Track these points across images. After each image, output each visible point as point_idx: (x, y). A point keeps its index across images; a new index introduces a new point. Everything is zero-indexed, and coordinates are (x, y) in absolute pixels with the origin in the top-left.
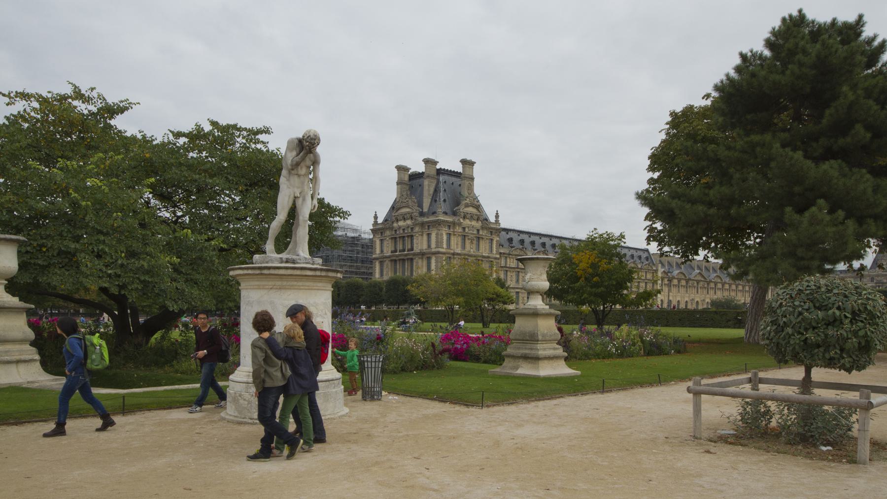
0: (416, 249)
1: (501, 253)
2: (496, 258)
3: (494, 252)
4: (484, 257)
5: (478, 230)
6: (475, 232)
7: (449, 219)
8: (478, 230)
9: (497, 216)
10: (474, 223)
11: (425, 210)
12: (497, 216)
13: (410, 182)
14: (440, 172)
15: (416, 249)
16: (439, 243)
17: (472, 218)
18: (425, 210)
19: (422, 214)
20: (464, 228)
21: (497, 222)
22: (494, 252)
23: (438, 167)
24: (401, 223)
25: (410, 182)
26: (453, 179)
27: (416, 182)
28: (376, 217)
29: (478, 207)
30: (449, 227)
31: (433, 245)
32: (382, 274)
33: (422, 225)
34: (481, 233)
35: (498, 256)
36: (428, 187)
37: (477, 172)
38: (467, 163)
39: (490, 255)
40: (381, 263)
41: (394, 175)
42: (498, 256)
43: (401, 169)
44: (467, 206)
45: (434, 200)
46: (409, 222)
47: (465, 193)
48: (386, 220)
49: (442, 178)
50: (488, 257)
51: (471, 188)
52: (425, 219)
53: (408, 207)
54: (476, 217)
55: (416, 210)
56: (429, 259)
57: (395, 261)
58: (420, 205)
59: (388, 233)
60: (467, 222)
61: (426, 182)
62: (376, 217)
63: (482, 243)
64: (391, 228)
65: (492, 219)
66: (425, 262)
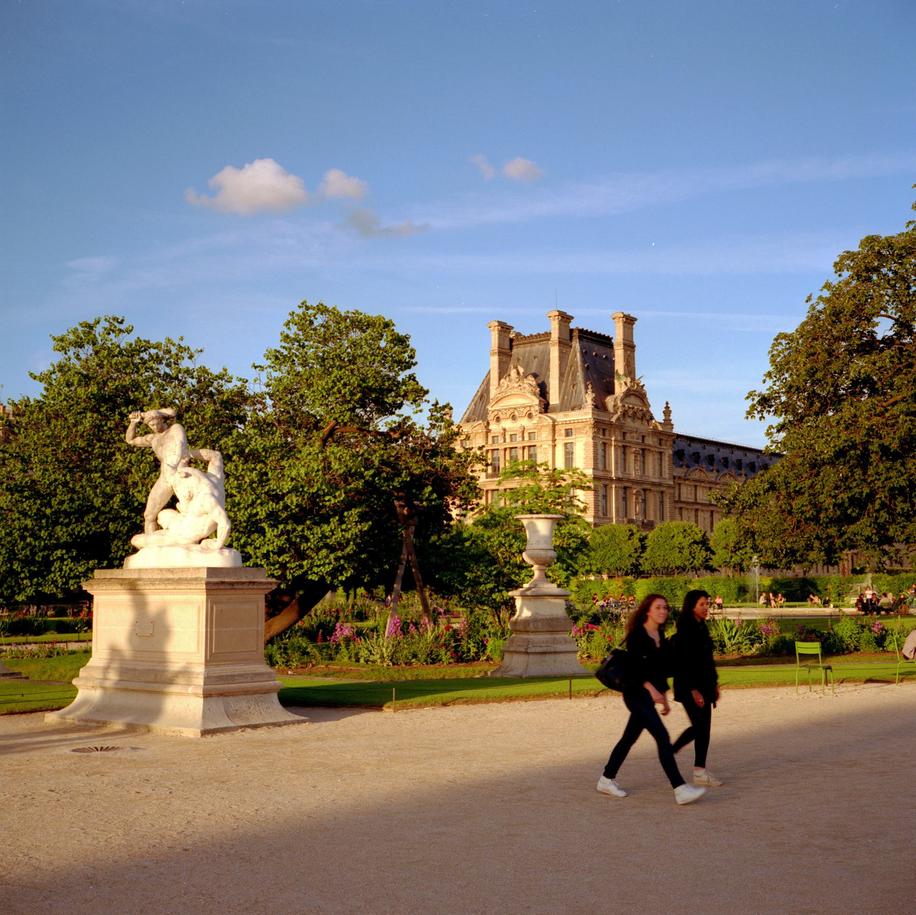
1: (674, 478)
2: (669, 487)
3: (667, 476)
4: (654, 484)
5: (643, 437)
6: (640, 441)
8: (643, 437)
9: (667, 412)
10: (637, 424)
12: (667, 412)
18: (554, 398)
20: (624, 433)
21: (668, 422)
22: (666, 474)
23: (573, 325)
24: (507, 424)
30: (604, 430)
34: (650, 441)
35: (671, 483)
39: (662, 481)
42: (671, 483)
50: (660, 485)
53: (524, 396)
54: (639, 414)
58: (543, 392)
63: (651, 460)
65: (659, 417)
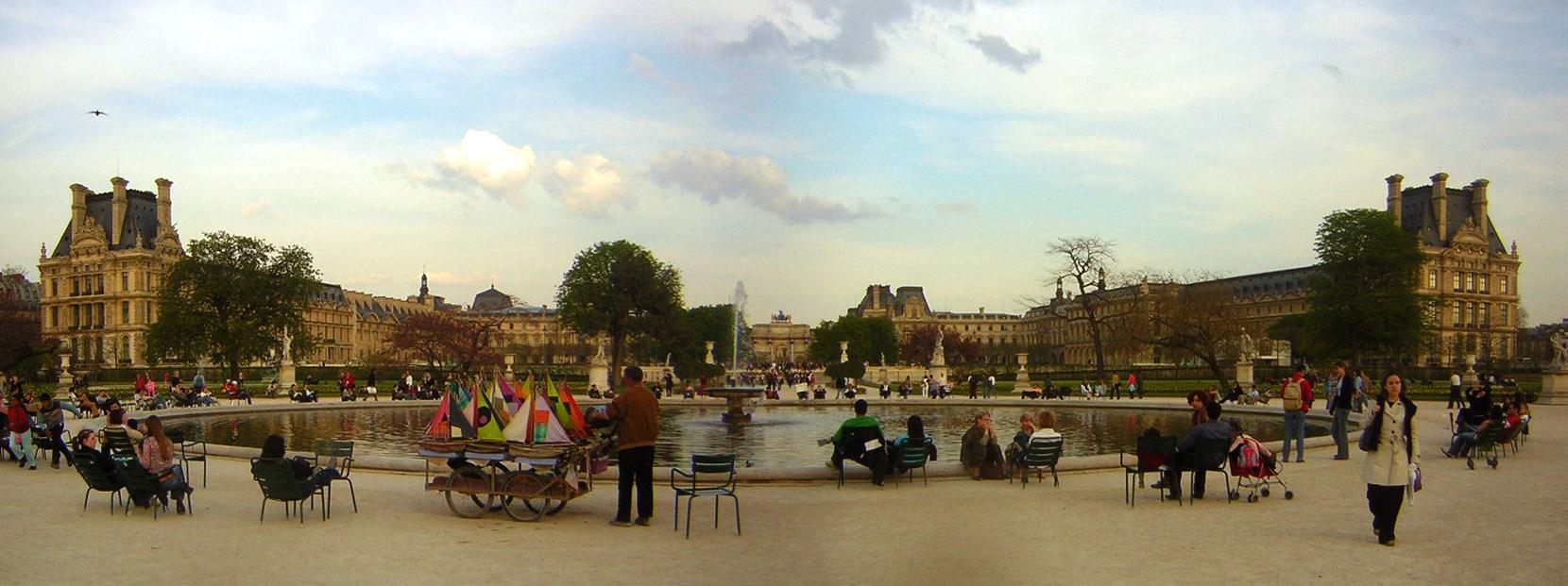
0: (108, 293)
7: (149, 254)
11: (116, 242)
13: (90, 204)
14: (132, 194)
15: (108, 293)
16: (139, 285)
17: (170, 253)
18: (116, 242)
19: (111, 247)
24: (83, 259)
25: (90, 204)
26: (144, 203)
27: (96, 206)
28: (44, 250)
29: (176, 238)
31: (131, 286)
32: (55, 323)
33: (116, 261)
36: (117, 212)
37: (174, 193)
38: (164, 184)
40: (55, 310)
41: (68, 198)
43: (78, 189)
44: (166, 237)
45: (126, 230)
46: (95, 258)
47: (160, 218)
48: (56, 254)
49: (135, 201)
51: (167, 214)
52: (119, 255)
55: (103, 244)
56: (126, 304)
57: (77, 307)
58: (109, 237)
59: (64, 271)
60: (166, 258)
61: (115, 208)
62: (44, 250)
64: (69, 265)
66: (119, 308)
